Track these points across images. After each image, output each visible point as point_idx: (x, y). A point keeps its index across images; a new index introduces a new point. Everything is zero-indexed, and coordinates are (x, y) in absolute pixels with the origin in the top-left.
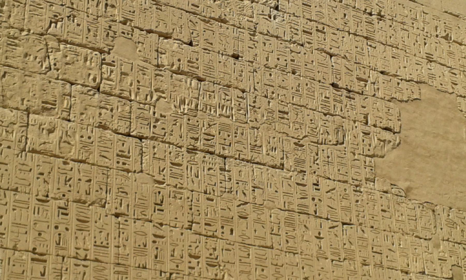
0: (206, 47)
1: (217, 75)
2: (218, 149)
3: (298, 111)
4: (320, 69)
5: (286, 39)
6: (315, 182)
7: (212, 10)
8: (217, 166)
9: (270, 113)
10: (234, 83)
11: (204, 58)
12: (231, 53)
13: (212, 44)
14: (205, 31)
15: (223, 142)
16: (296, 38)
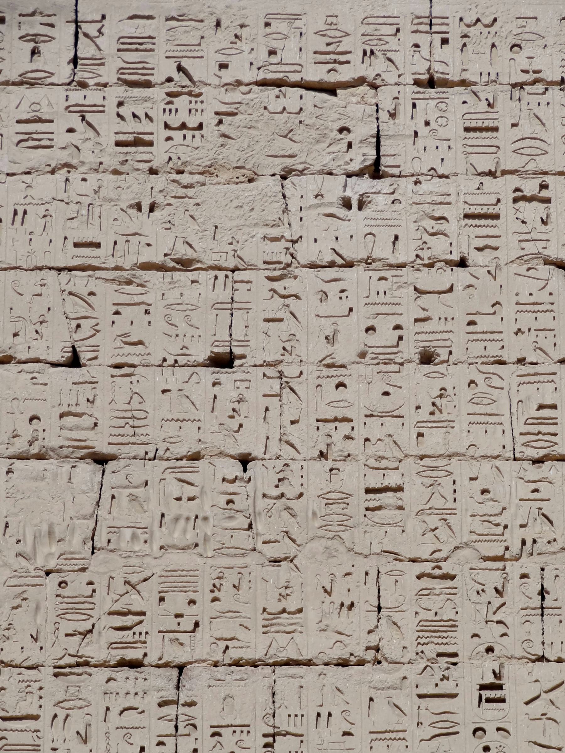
0: (119, 360)
1: (155, 434)
2: (155, 649)
3: (434, 474)
4: (526, 321)
5: (401, 259)
6: (490, 679)
7: (144, 240)
8: (154, 698)
9: (336, 501)
10: (215, 440)
11: (113, 393)
12: (202, 356)
13: (140, 343)
14: (117, 313)
15: (172, 623)
16: (439, 248)
